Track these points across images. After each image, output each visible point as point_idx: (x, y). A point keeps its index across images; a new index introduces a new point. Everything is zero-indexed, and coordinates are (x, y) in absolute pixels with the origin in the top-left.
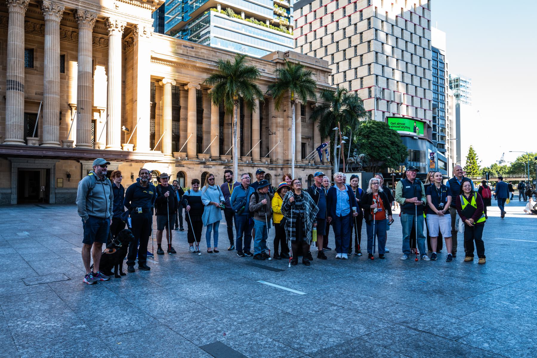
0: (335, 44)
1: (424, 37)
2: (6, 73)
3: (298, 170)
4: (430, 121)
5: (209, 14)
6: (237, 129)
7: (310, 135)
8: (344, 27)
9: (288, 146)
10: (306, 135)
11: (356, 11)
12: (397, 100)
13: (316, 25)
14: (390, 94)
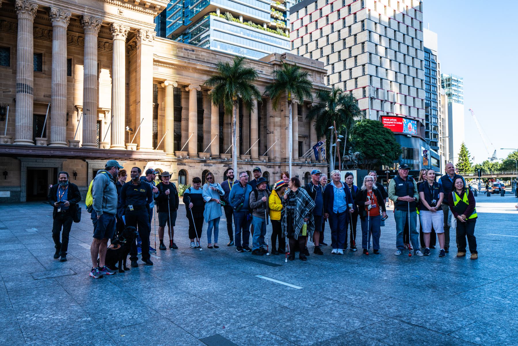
0: (330, 46)
1: (416, 38)
2: (15, 77)
3: (295, 168)
4: (423, 120)
5: (209, 17)
6: (237, 128)
7: (307, 134)
8: (339, 29)
9: (285, 144)
10: (304, 134)
11: (350, 14)
12: (391, 100)
13: (312, 27)
14: (384, 94)
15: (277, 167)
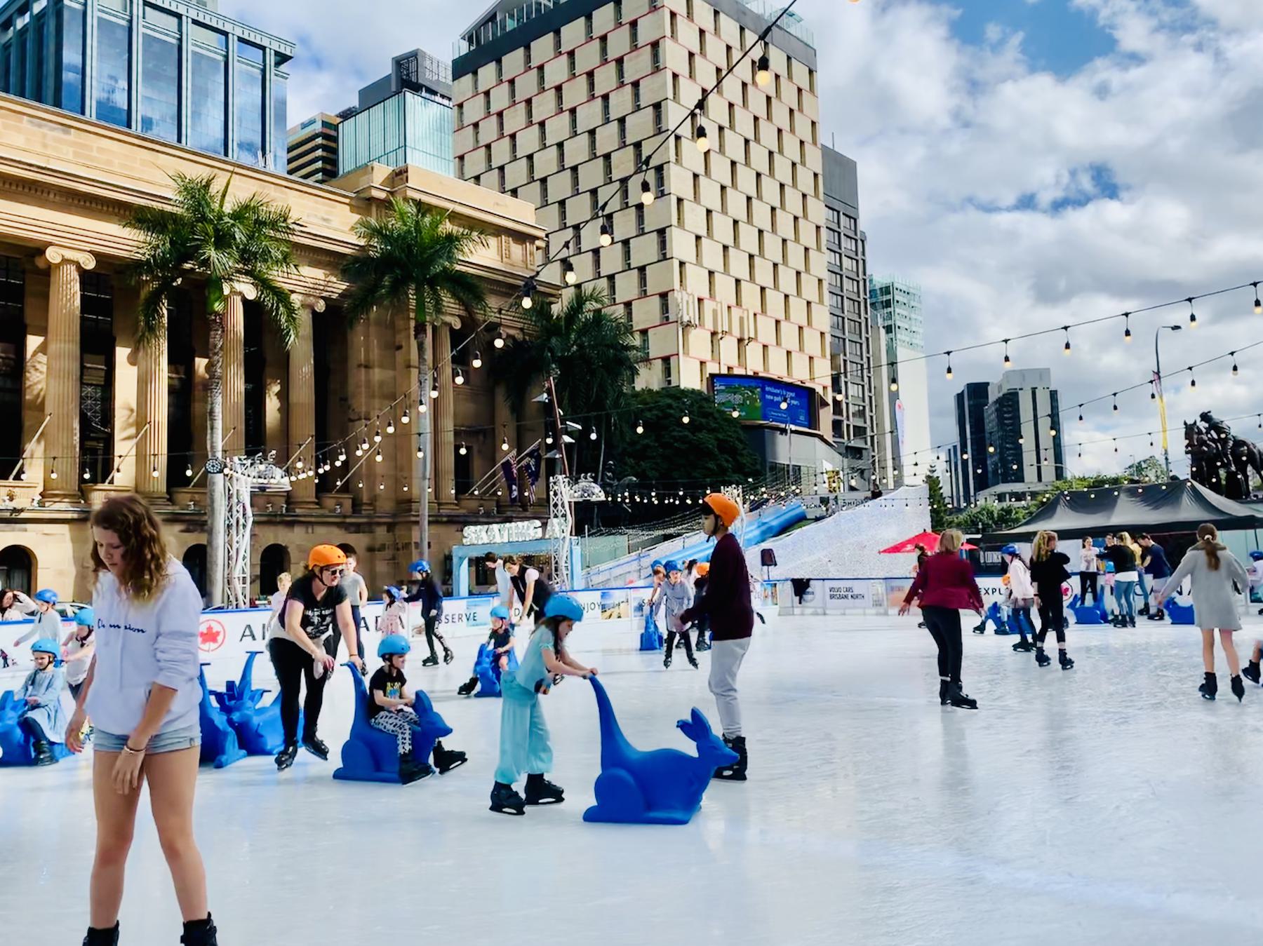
11: (622, 85)
15: (385, 528)
